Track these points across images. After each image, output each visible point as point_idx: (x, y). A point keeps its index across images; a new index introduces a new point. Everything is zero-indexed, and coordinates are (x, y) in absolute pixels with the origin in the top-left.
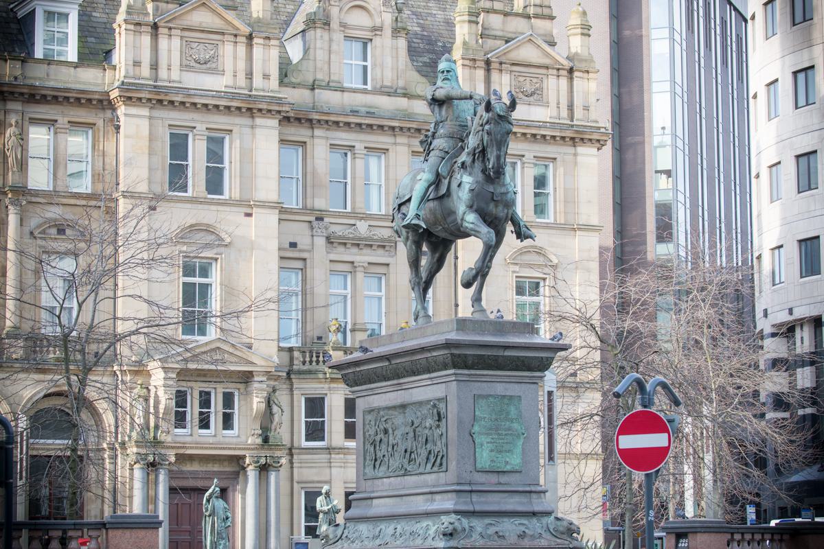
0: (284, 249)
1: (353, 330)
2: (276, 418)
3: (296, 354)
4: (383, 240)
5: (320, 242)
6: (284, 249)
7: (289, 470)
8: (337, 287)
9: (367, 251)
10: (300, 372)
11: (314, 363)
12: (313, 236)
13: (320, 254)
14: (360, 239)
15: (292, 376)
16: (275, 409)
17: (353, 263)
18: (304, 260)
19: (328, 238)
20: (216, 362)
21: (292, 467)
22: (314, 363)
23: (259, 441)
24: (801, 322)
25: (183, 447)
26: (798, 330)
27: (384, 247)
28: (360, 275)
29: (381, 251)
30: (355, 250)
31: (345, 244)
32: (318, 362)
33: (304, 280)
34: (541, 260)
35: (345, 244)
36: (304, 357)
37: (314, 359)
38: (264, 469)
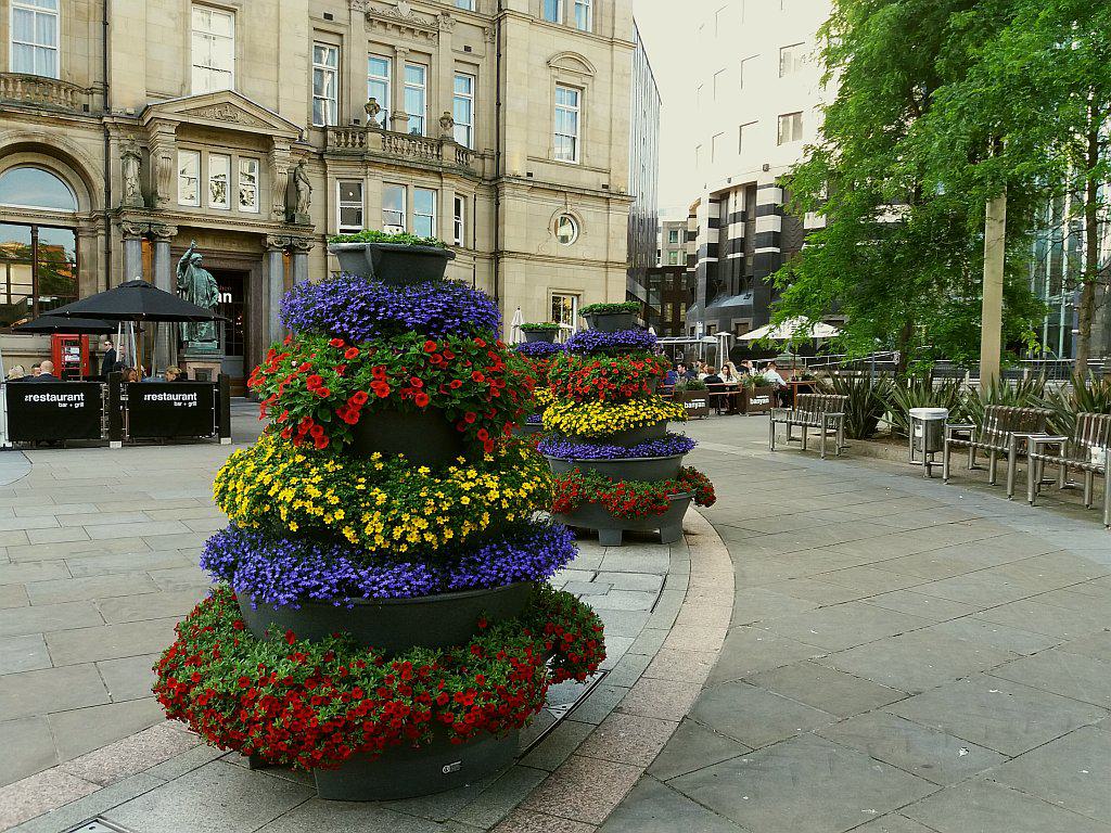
0: (318, 20)
1: (391, 119)
2: (303, 195)
3: (330, 134)
4: (424, 26)
5: (359, 17)
6: (318, 20)
7: (321, 254)
8: (376, 71)
9: (408, 35)
10: (334, 154)
11: (350, 145)
12: (350, 10)
13: (358, 31)
14: (401, 21)
15: (325, 157)
16: (302, 185)
17: (393, 47)
18: (341, 35)
19: (367, 15)
20: (232, 119)
21: (326, 256)
22: (350, 145)
23: (282, 218)
24: (736, 189)
25: (188, 219)
26: (732, 196)
27: (426, 34)
28: (401, 61)
29: (422, 39)
30: (395, 32)
31: (385, 24)
32: (354, 145)
33: (341, 59)
34: (581, 69)
35: (385, 24)
36: (339, 140)
37: (350, 140)
38: (291, 251)
